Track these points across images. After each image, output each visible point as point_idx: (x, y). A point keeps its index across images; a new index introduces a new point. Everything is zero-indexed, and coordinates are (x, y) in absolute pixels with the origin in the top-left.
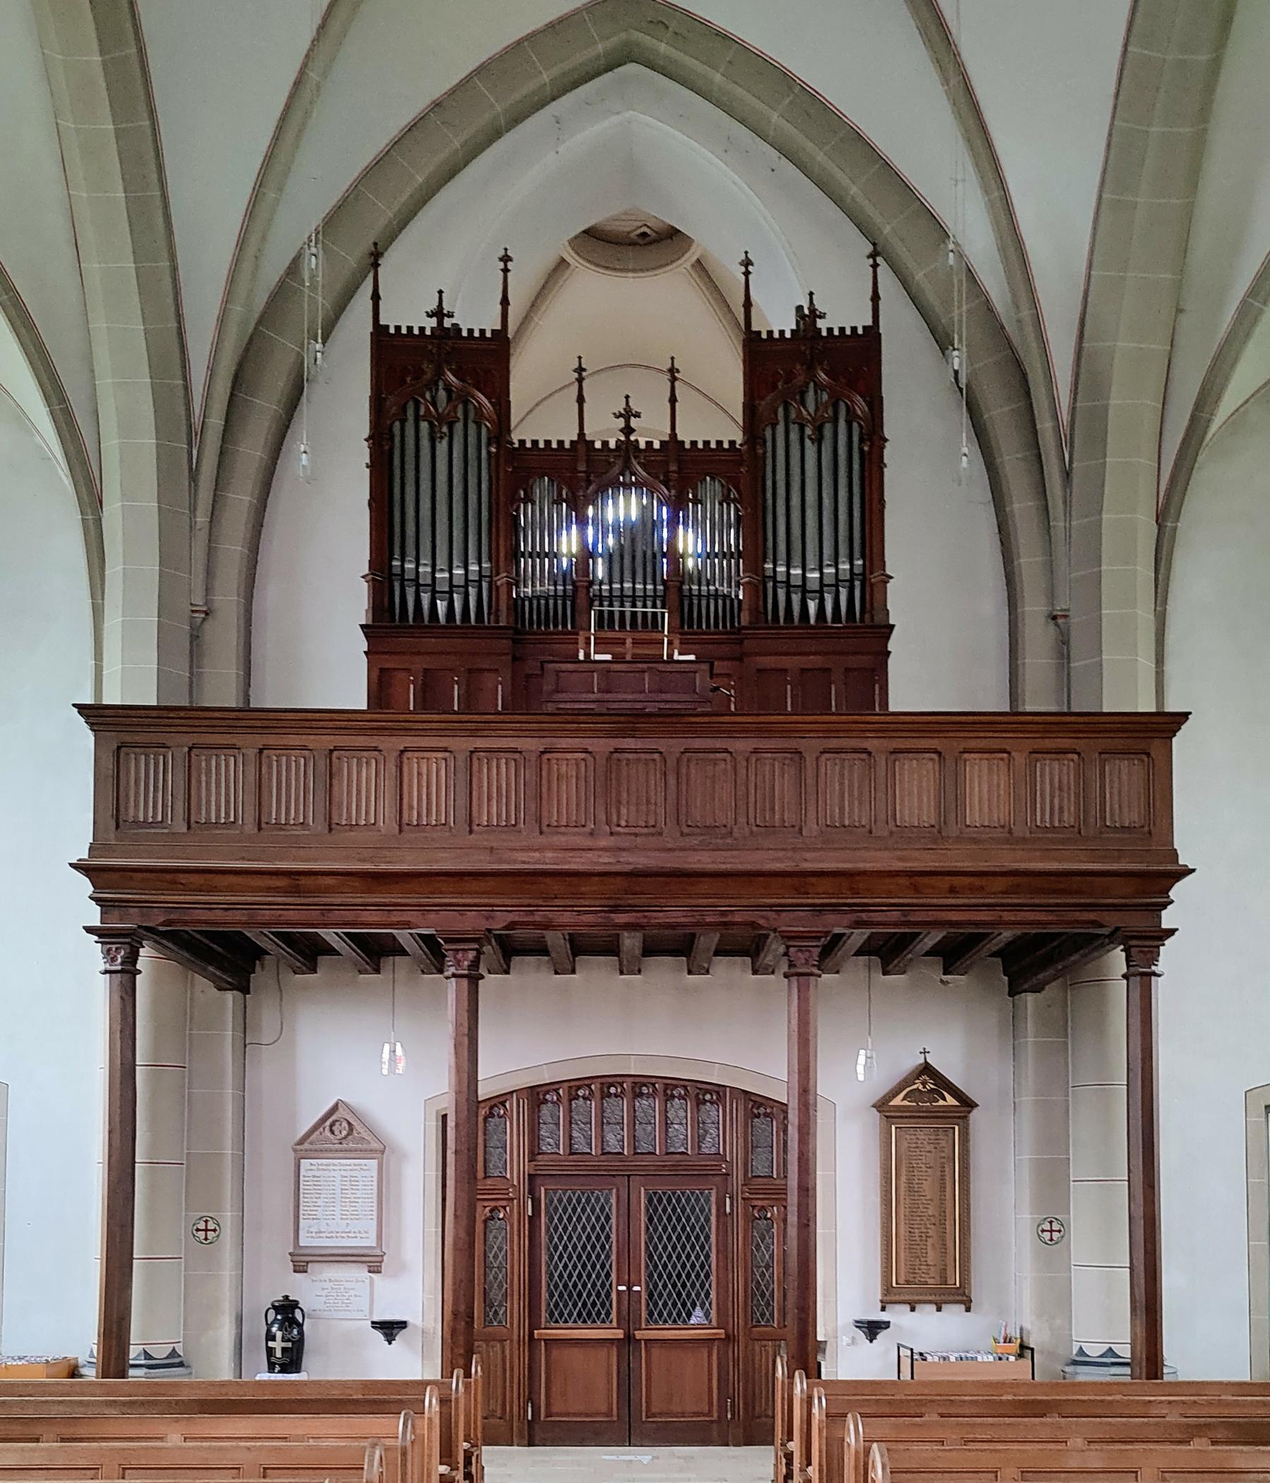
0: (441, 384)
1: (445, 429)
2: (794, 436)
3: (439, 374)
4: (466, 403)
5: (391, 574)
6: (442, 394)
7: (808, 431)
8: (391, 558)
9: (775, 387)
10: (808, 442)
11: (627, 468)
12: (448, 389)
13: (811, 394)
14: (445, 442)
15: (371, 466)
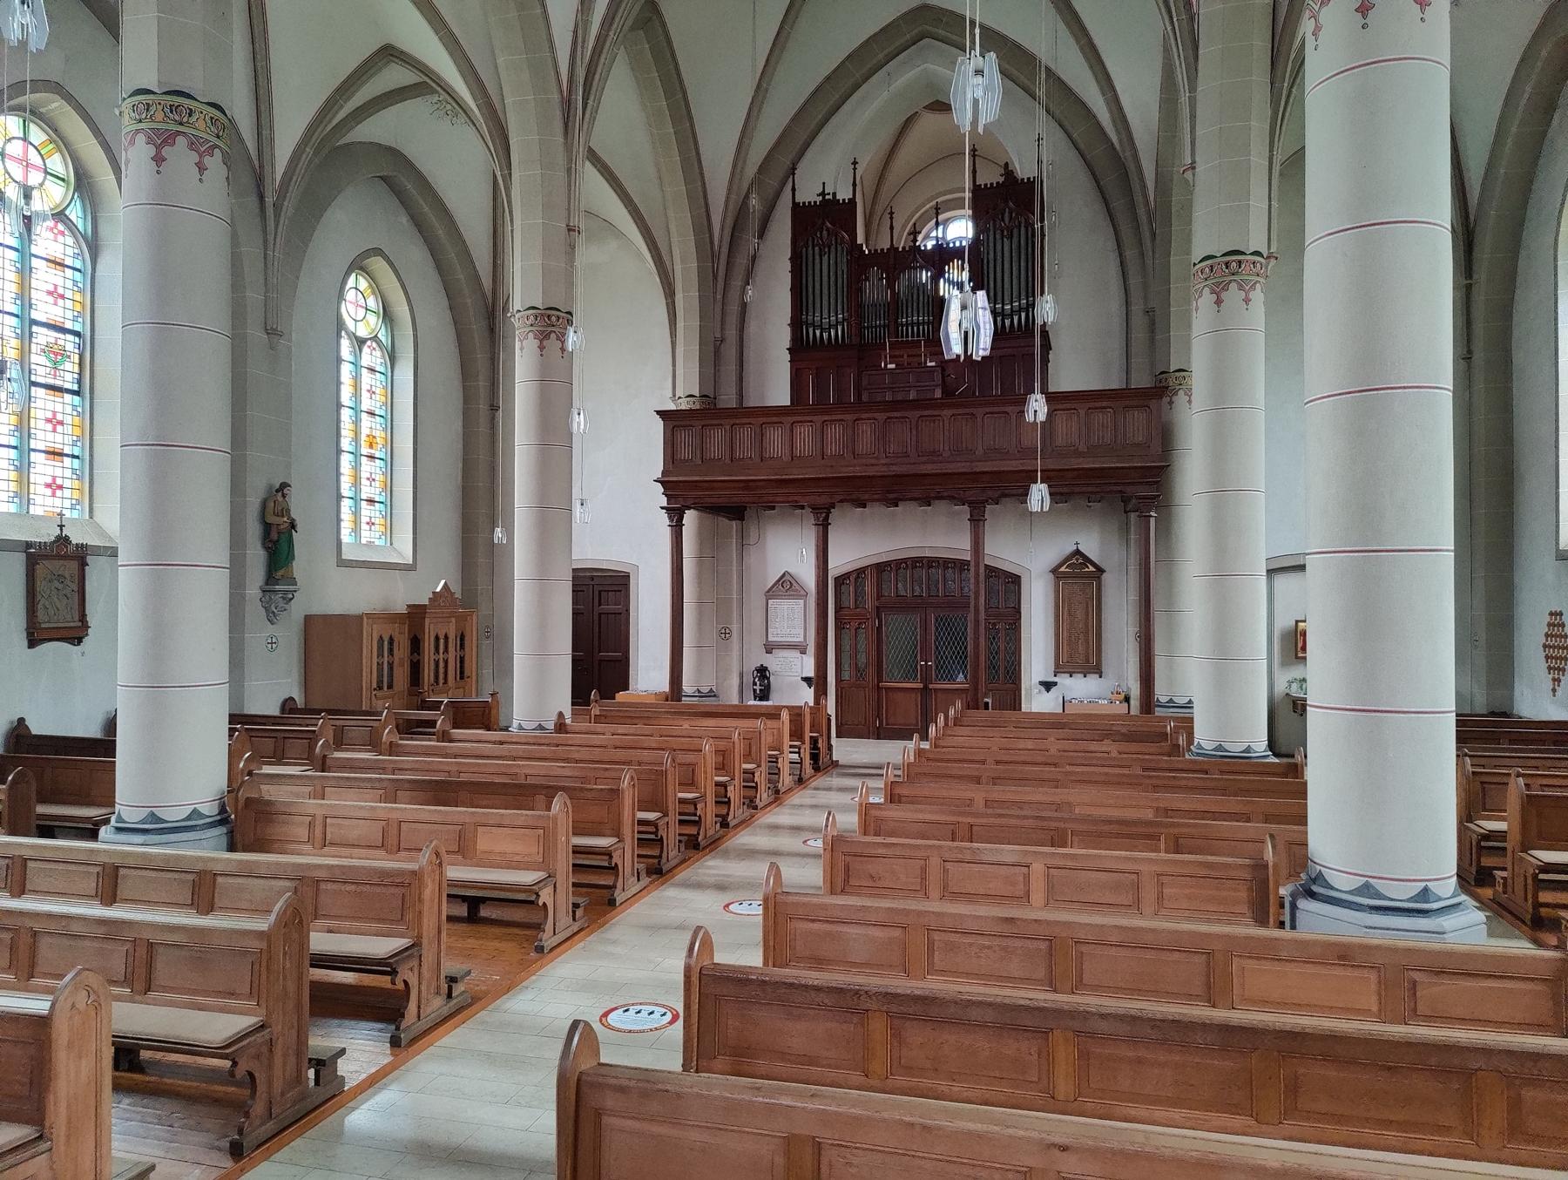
0: (825, 228)
1: (826, 250)
2: (998, 237)
3: (824, 223)
4: (836, 236)
5: (801, 321)
6: (825, 232)
7: (1005, 233)
8: (802, 314)
9: (988, 213)
10: (1005, 239)
11: (915, 260)
12: (828, 230)
13: (1007, 214)
14: (826, 256)
15: (792, 272)
